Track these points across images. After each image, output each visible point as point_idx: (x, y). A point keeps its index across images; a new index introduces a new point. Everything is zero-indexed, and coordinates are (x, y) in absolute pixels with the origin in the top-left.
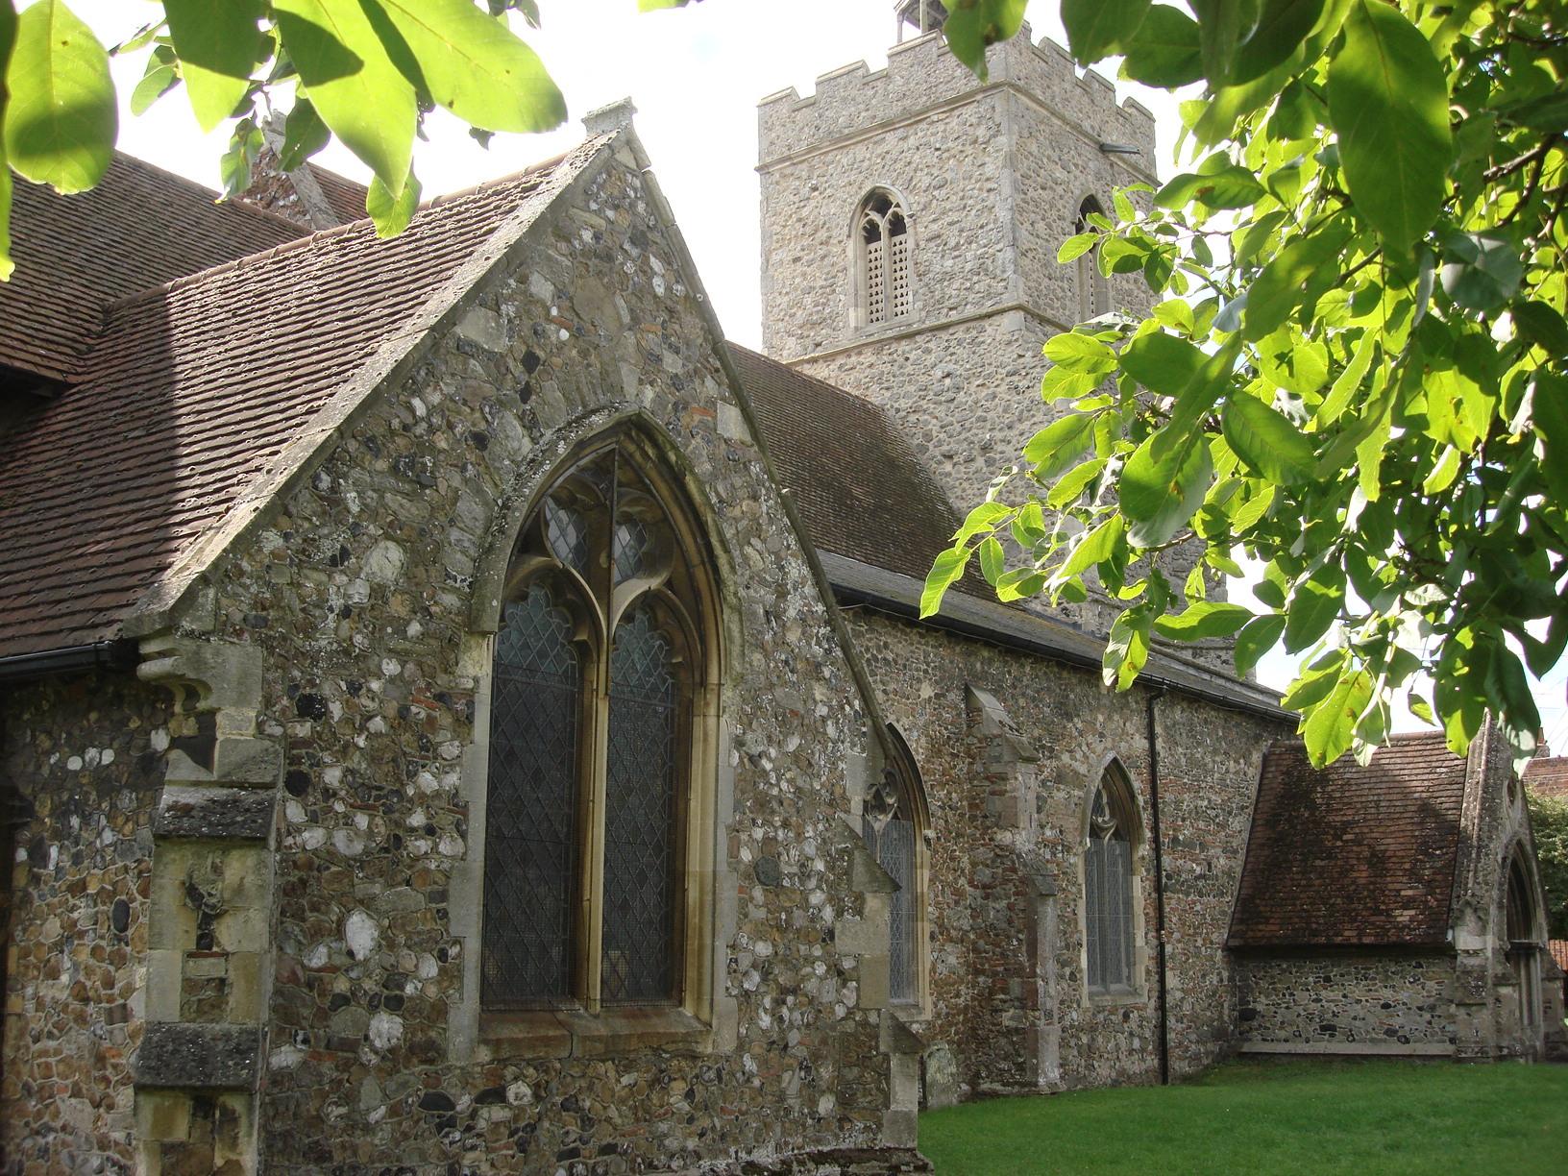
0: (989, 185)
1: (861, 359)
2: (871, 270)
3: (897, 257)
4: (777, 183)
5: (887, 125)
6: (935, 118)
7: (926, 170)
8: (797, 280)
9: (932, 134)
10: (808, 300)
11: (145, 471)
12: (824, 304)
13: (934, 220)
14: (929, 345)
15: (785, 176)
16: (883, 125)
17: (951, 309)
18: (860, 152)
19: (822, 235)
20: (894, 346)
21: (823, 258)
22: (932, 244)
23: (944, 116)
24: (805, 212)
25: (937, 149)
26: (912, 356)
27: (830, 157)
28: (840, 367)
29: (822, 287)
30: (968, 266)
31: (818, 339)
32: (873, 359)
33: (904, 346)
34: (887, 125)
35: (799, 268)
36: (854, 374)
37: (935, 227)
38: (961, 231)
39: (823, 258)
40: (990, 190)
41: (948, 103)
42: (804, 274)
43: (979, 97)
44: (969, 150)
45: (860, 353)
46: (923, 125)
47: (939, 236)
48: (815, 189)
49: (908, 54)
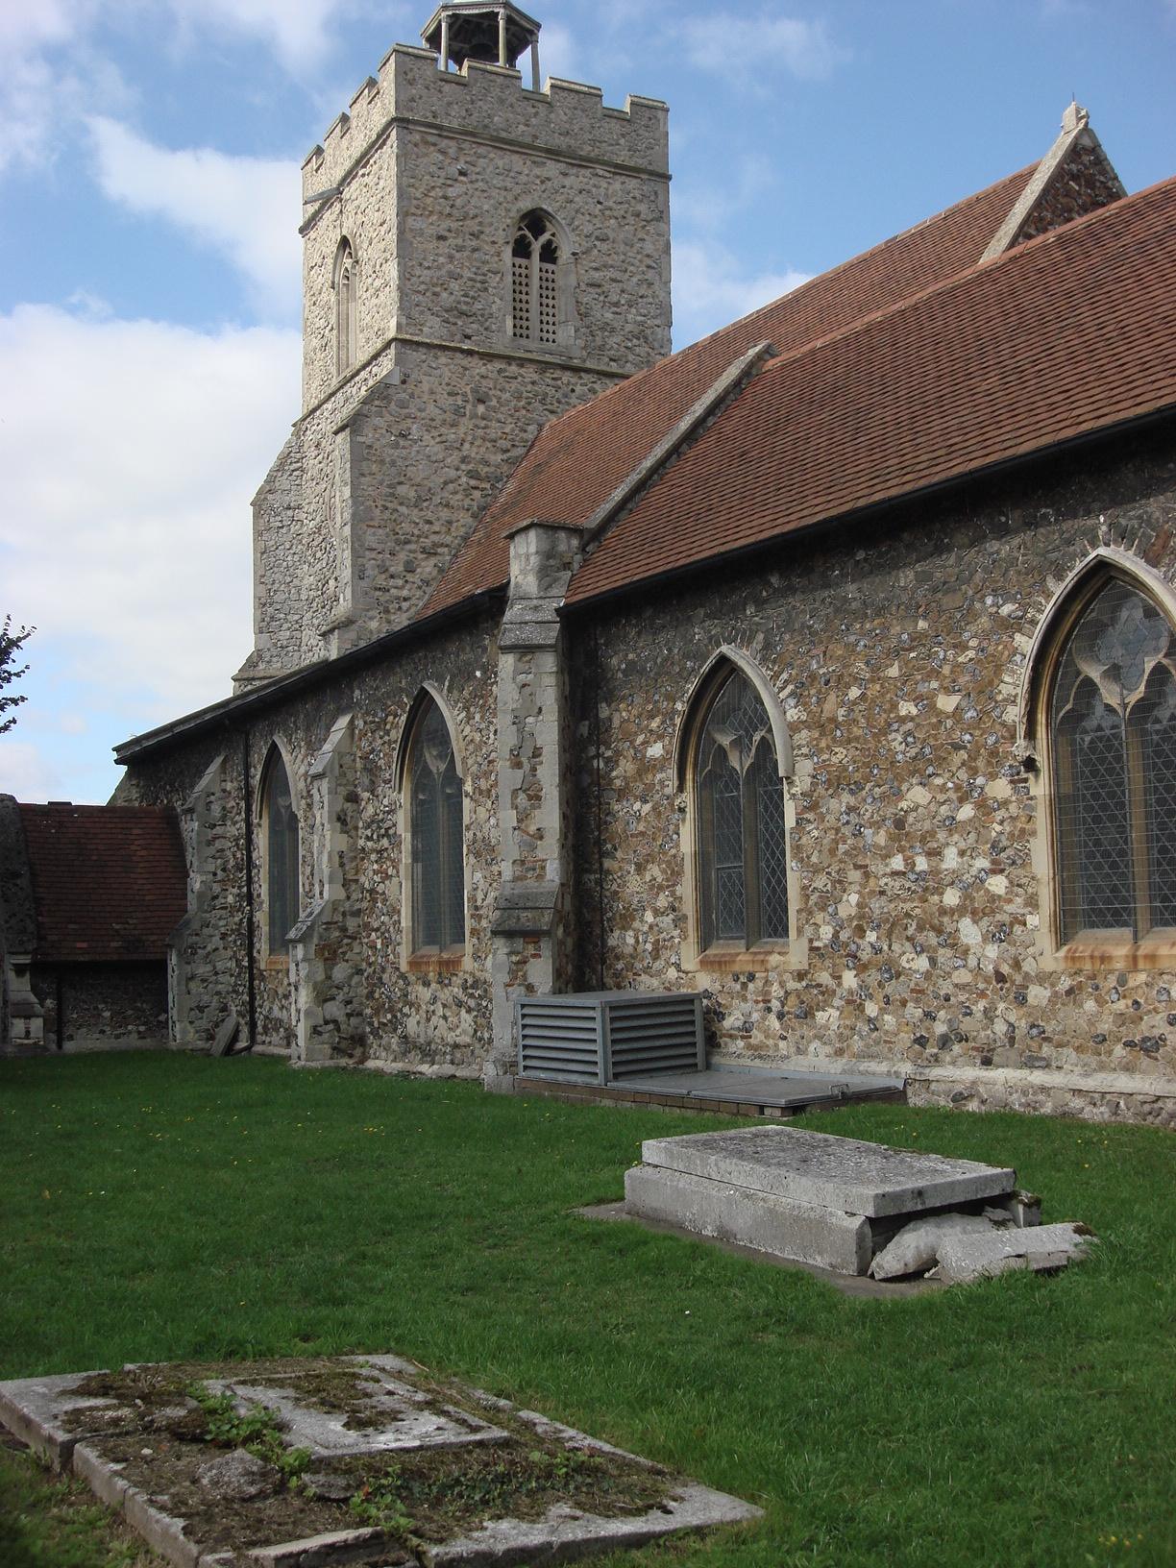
0: (650, 262)
1: (522, 371)
2: (520, 284)
3: (548, 285)
4: (416, 145)
5: (553, 153)
6: (601, 173)
7: (588, 217)
8: (442, 260)
9: (595, 186)
10: (454, 285)
11: (934, 463)
12: (473, 297)
13: (596, 269)
14: (595, 385)
15: (426, 143)
16: (548, 151)
17: (611, 360)
18: (517, 162)
19: (472, 225)
20: (558, 373)
21: (474, 250)
22: (590, 290)
23: (608, 175)
24: (451, 192)
25: (599, 203)
26: (578, 389)
27: (482, 150)
28: (500, 371)
29: (471, 279)
30: (629, 327)
31: (469, 332)
32: (536, 377)
33: (567, 377)
34: (553, 153)
35: (444, 248)
36: (514, 385)
37: (597, 275)
38: (623, 291)
39: (474, 250)
40: (649, 267)
41: (617, 166)
42: (451, 257)
43: (643, 176)
44: (631, 219)
45: (522, 366)
46: (587, 172)
47: (599, 286)
48: (462, 173)
49: (572, 95)
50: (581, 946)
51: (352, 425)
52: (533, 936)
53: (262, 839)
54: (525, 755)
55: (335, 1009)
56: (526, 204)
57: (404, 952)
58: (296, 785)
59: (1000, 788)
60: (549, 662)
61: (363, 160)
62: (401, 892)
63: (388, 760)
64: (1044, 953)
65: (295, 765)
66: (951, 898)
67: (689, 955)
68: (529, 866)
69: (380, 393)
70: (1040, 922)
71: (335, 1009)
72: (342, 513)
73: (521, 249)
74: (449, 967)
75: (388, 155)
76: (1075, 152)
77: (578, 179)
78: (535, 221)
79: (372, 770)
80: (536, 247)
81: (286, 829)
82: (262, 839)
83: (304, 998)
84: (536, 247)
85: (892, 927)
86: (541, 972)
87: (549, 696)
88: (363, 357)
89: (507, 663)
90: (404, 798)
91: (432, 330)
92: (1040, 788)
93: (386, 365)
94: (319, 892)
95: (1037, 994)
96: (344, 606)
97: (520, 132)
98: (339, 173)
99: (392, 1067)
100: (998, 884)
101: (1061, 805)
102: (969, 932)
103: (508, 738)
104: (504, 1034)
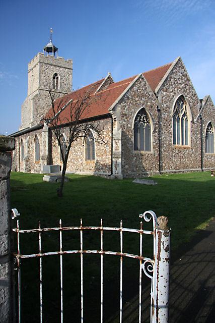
5: (58, 66)
50: (50, 161)
51: (33, 99)
52: (45, 159)
53: (21, 148)
54: (44, 142)
55: (27, 167)
56: (55, 72)
57: (34, 161)
58: (24, 143)
59: (82, 147)
60: (47, 133)
61: (35, 66)
62: (34, 155)
63: (33, 141)
64: (84, 162)
65: (24, 141)
66: (78, 157)
67: (59, 162)
68: (45, 153)
69: (37, 95)
70: (84, 159)
71: (27, 167)
72: (32, 110)
73: (54, 78)
74: (39, 162)
75: (38, 66)
76: (109, 77)
77: (62, 69)
78: (56, 74)
79: (32, 142)
80: (56, 78)
81: (23, 147)
82: (21, 148)
83: (24, 166)
84: (56, 78)
85: (74, 159)
86: (46, 163)
87: (47, 137)
88: (34, 90)
89: (43, 133)
90: (34, 145)
91: (43, 88)
92: (84, 148)
93: (37, 92)
94: (26, 155)
95: (84, 165)
96: (32, 121)
97: (54, 64)
98: (32, 67)
99: (33, 173)
100: (81, 156)
101: (86, 149)
102: (79, 160)
103: (43, 140)
104: (42, 169)
